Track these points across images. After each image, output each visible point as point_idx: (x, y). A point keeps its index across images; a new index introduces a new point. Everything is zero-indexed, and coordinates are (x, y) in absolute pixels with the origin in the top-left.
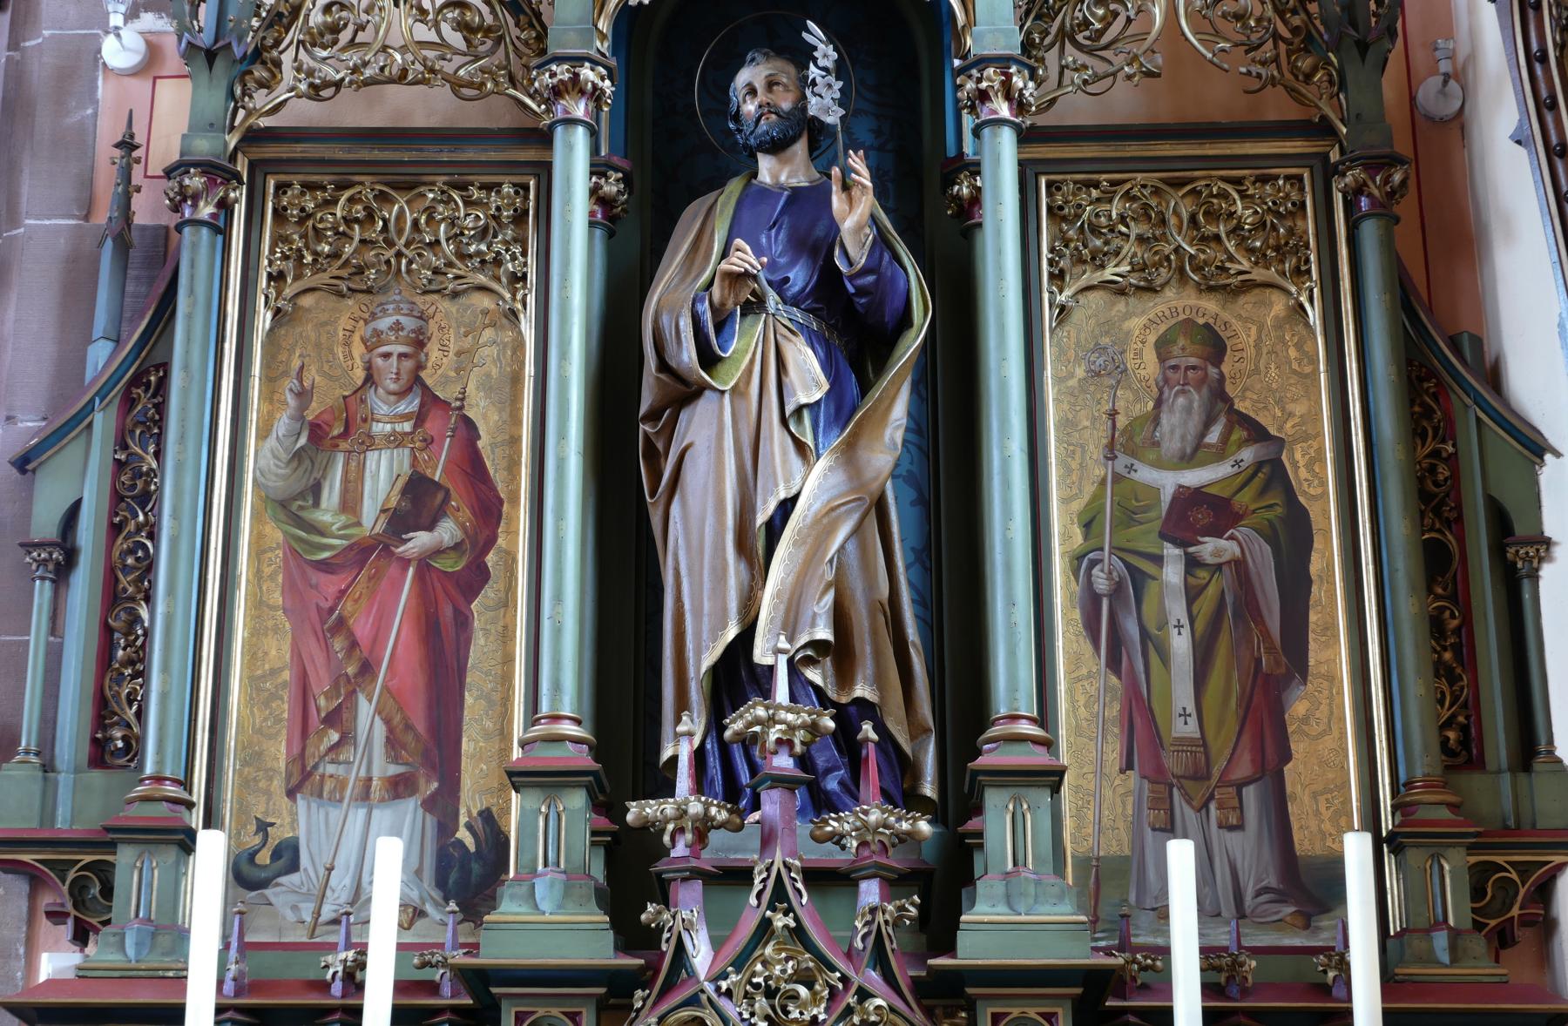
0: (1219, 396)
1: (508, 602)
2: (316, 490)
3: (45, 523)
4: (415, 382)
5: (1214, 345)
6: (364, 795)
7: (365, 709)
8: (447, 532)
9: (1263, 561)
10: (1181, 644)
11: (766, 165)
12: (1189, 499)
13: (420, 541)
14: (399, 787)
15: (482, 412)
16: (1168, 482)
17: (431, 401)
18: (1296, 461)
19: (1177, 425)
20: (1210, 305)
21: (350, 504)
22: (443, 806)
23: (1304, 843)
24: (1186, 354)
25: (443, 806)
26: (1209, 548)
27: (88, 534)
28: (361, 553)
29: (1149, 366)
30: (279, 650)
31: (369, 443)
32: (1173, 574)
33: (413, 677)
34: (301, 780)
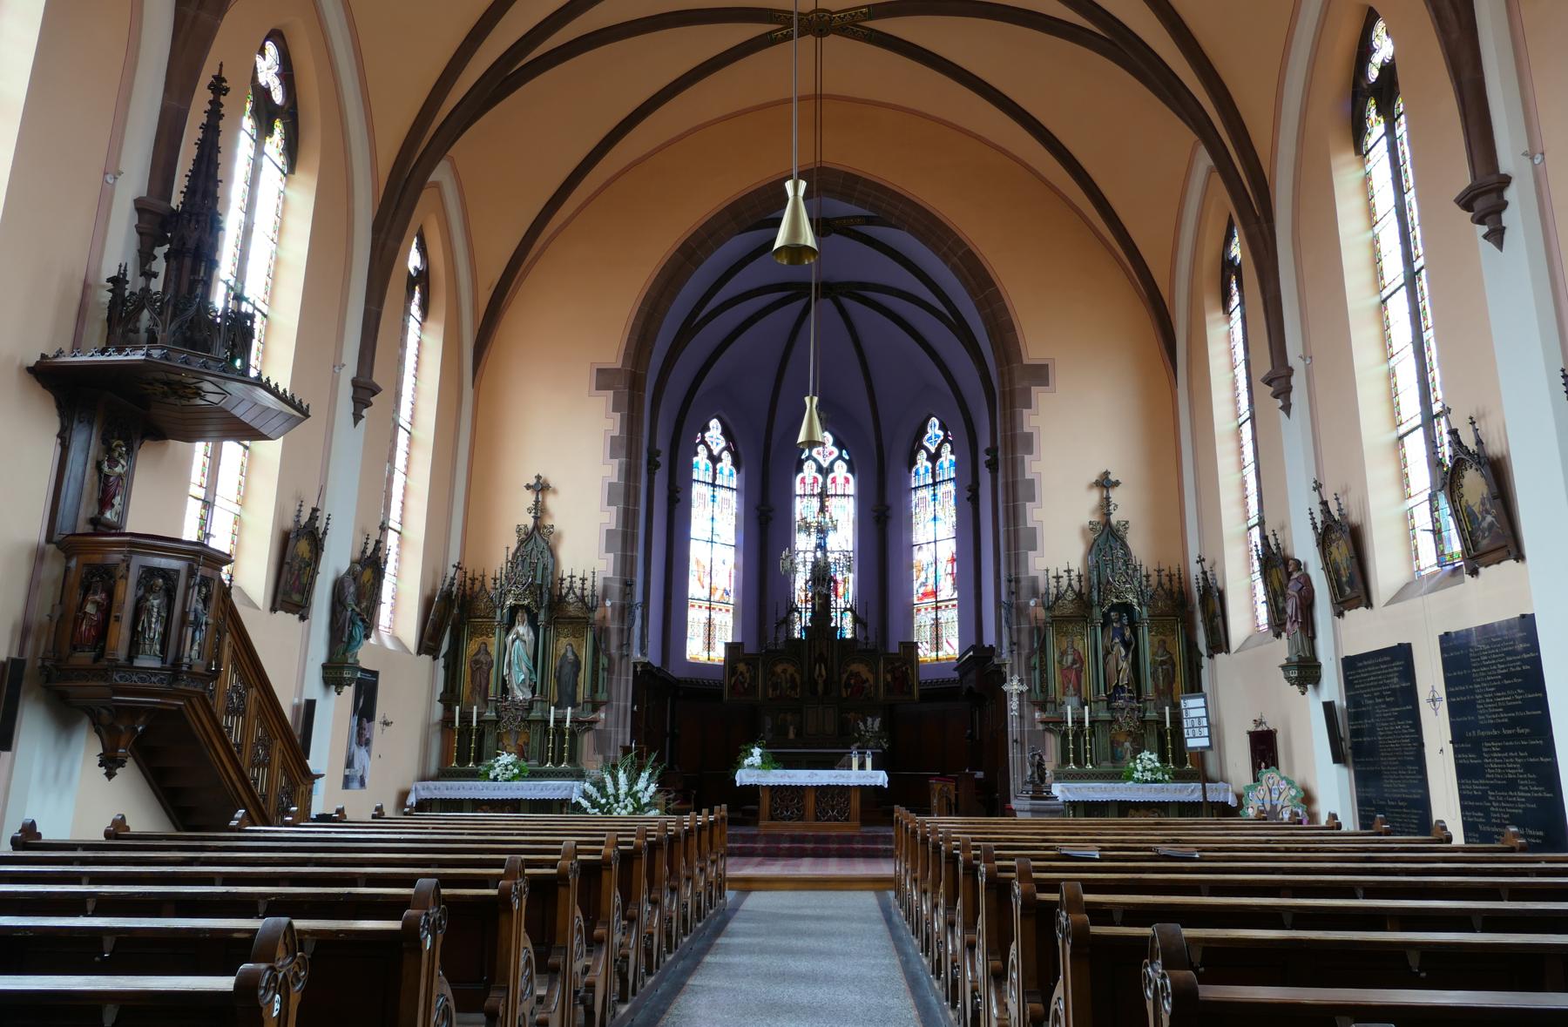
0: (1165, 648)
1: (1085, 673)
2: (1062, 660)
3: (1033, 663)
4: (1073, 647)
5: (1164, 642)
6: (1071, 696)
7: (1071, 686)
8: (1078, 665)
9: (1170, 669)
10: (1161, 678)
11: (1114, 624)
12: (1161, 661)
13: (1075, 666)
14: (1075, 695)
15: (1081, 652)
16: (1159, 659)
17: (1075, 650)
18: (1174, 656)
19: (1160, 652)
20: (1164, 638)
21: (1067, 662)
22: (1080, 697)
23: (1175, 701)
24: (1161, 643)
25: (1080, 697)
26: (1164, 667)
27: (1037, 666)
28: (1068, 667)
29: (1157, 645)
30: (1061, 679)
31: (1068, 655)
32: (1160, 670)
33: (1076, 681)
34: (1064, 694)
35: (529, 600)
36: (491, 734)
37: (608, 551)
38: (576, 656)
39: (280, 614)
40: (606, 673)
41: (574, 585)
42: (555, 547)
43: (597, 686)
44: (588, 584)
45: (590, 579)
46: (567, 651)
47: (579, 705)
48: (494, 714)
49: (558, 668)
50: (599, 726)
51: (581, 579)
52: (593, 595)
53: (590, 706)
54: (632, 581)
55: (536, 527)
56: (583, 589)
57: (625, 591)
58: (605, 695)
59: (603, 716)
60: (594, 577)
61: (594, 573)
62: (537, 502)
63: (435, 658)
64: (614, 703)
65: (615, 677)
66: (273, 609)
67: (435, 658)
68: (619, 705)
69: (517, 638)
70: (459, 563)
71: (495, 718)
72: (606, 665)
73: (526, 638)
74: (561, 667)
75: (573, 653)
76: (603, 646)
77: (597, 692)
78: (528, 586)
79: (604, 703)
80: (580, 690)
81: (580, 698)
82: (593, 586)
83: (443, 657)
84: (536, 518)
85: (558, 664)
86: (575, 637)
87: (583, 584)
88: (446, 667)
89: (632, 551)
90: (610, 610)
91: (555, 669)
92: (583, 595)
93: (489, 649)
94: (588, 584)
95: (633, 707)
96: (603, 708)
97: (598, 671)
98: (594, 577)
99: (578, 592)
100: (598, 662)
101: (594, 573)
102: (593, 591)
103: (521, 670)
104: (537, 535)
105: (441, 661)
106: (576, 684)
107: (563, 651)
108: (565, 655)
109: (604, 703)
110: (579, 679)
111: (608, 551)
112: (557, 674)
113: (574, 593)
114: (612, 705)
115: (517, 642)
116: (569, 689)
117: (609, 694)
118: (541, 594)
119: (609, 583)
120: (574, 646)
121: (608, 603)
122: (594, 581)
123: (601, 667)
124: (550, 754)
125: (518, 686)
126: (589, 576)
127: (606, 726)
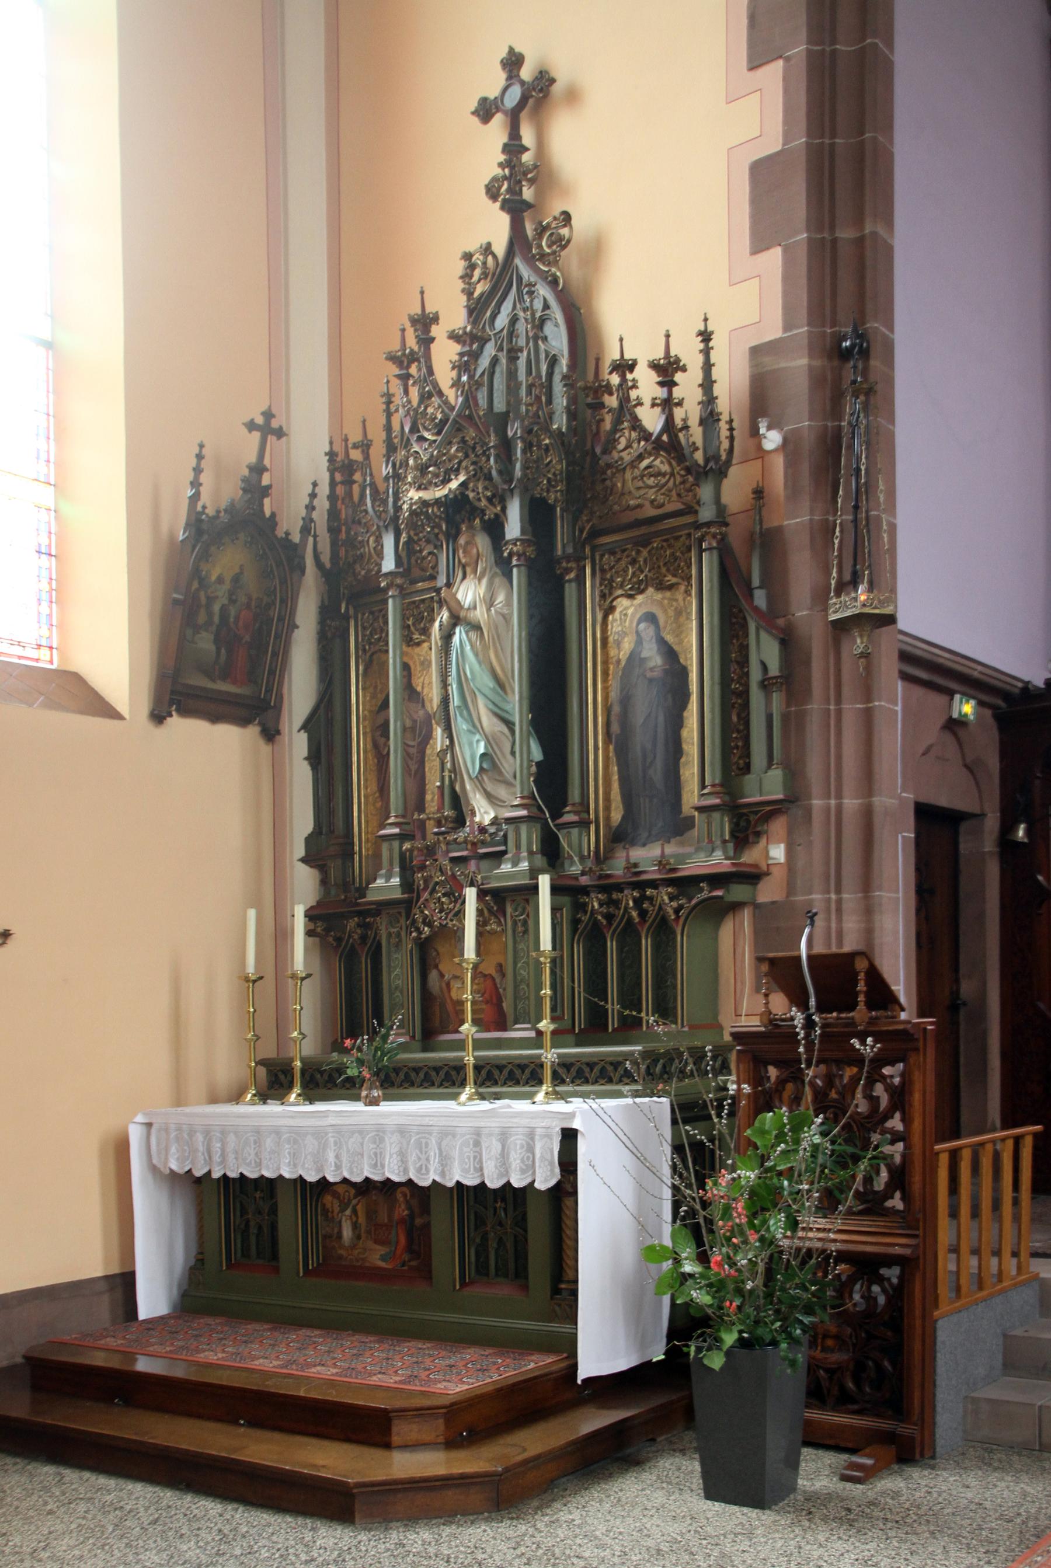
35: (462, 478)
36: (398, 945)
37: (759, 245)
38: (671, 654)
39: (176, 722)
40: (777, 699)
41: (633, 394)
42: (588, 291)
43: (746, 752)
44: (688, 386)
45: (693, 360)
46: (639, 641)
47: (689, 824)
48: (396, 881)
49: (616, 709)
50: (768, 892)
51: (654, 366)
52: (710, 418)
53: (723, 825)
54: (860, 335)
55: (518, 240)
56: (668, 404)
57: (838, 380)
58: (776, 775)
59: (778, 853)
60: (706, 352)
61: (706, 336)
62: (513, 148)
63: (271, 734)
64: (817, 803)
65: (814, 707)
66: (158, 717)
67: (271, 734)
68: (839, 809)
69: (456, 620)
70: (268, 415)
71: (398, 895)
72: (774, 670)
73: (480, 615)
74: (626, 701)
75: (662, 642)
76: (760, 599)
77: (747, 769)
78: (458, 428)
79: (772, 811)
80: (690, 772)
81: (691, 796)
82: (708, 384)
83: (305, 727)
84: (516, 209)
85: (614, 695)
86: (661, 587)
87: (668, 383)
88: (314, 758)
89: (859, 221)
90: (779, 463)
91: (608, 710)
92: (669, 425)
93: (418, 684)
94: (688, 386)
95: (1007, 827)
96: (778, 826)
97: (745, 694)
98: (706, 352)
99: (652, 420)
100: (744, 662)
101: (706, 336)
102: (709, 400)
103: (475, 726)
104: (526, 272)
105: (298, 744)
106: (675, 750)
107: (627, 645)
108: (634, 658)
109: (772, 811)
110: (685, 733)
111: (759, 245)
112: (615, 728)
113: (636, 424)
114: (808, 811)
115: (459, 635)
116: (657, 773)
117: (794, 774)
118: (506, 446)
119: (770, 363)
120: (661, 619)
121: (772, 440)
122: (708, 367)
123: (755, 675)
124: (547, 991)
125: (478, 781)
126: (688, 351)
127: (791, 889)
